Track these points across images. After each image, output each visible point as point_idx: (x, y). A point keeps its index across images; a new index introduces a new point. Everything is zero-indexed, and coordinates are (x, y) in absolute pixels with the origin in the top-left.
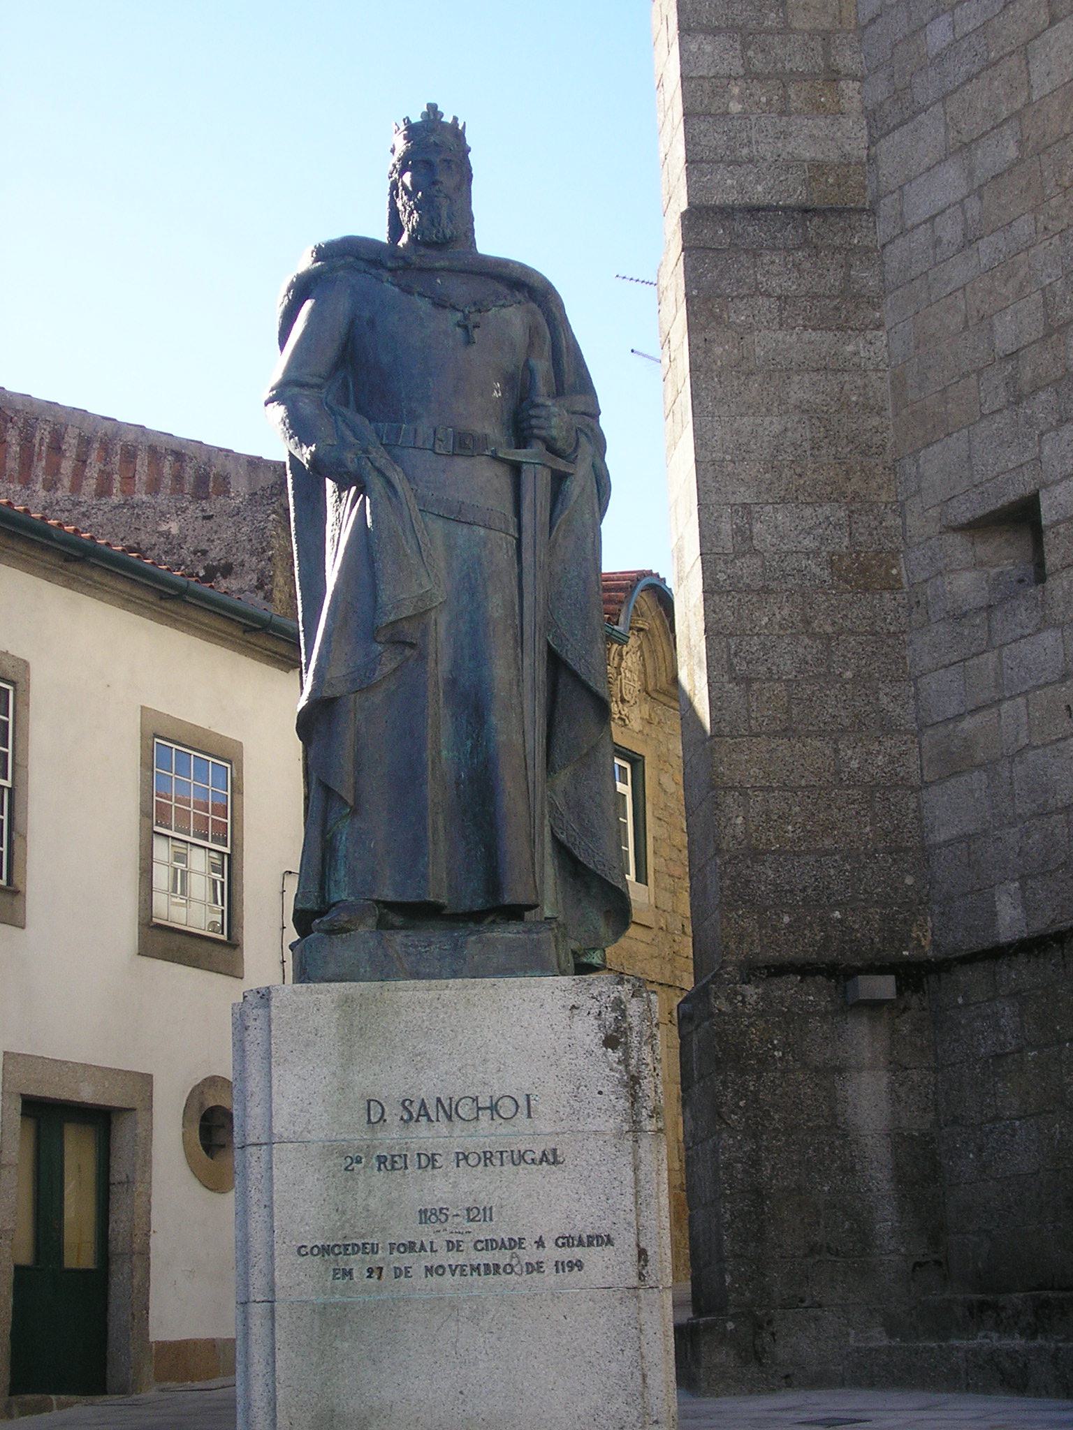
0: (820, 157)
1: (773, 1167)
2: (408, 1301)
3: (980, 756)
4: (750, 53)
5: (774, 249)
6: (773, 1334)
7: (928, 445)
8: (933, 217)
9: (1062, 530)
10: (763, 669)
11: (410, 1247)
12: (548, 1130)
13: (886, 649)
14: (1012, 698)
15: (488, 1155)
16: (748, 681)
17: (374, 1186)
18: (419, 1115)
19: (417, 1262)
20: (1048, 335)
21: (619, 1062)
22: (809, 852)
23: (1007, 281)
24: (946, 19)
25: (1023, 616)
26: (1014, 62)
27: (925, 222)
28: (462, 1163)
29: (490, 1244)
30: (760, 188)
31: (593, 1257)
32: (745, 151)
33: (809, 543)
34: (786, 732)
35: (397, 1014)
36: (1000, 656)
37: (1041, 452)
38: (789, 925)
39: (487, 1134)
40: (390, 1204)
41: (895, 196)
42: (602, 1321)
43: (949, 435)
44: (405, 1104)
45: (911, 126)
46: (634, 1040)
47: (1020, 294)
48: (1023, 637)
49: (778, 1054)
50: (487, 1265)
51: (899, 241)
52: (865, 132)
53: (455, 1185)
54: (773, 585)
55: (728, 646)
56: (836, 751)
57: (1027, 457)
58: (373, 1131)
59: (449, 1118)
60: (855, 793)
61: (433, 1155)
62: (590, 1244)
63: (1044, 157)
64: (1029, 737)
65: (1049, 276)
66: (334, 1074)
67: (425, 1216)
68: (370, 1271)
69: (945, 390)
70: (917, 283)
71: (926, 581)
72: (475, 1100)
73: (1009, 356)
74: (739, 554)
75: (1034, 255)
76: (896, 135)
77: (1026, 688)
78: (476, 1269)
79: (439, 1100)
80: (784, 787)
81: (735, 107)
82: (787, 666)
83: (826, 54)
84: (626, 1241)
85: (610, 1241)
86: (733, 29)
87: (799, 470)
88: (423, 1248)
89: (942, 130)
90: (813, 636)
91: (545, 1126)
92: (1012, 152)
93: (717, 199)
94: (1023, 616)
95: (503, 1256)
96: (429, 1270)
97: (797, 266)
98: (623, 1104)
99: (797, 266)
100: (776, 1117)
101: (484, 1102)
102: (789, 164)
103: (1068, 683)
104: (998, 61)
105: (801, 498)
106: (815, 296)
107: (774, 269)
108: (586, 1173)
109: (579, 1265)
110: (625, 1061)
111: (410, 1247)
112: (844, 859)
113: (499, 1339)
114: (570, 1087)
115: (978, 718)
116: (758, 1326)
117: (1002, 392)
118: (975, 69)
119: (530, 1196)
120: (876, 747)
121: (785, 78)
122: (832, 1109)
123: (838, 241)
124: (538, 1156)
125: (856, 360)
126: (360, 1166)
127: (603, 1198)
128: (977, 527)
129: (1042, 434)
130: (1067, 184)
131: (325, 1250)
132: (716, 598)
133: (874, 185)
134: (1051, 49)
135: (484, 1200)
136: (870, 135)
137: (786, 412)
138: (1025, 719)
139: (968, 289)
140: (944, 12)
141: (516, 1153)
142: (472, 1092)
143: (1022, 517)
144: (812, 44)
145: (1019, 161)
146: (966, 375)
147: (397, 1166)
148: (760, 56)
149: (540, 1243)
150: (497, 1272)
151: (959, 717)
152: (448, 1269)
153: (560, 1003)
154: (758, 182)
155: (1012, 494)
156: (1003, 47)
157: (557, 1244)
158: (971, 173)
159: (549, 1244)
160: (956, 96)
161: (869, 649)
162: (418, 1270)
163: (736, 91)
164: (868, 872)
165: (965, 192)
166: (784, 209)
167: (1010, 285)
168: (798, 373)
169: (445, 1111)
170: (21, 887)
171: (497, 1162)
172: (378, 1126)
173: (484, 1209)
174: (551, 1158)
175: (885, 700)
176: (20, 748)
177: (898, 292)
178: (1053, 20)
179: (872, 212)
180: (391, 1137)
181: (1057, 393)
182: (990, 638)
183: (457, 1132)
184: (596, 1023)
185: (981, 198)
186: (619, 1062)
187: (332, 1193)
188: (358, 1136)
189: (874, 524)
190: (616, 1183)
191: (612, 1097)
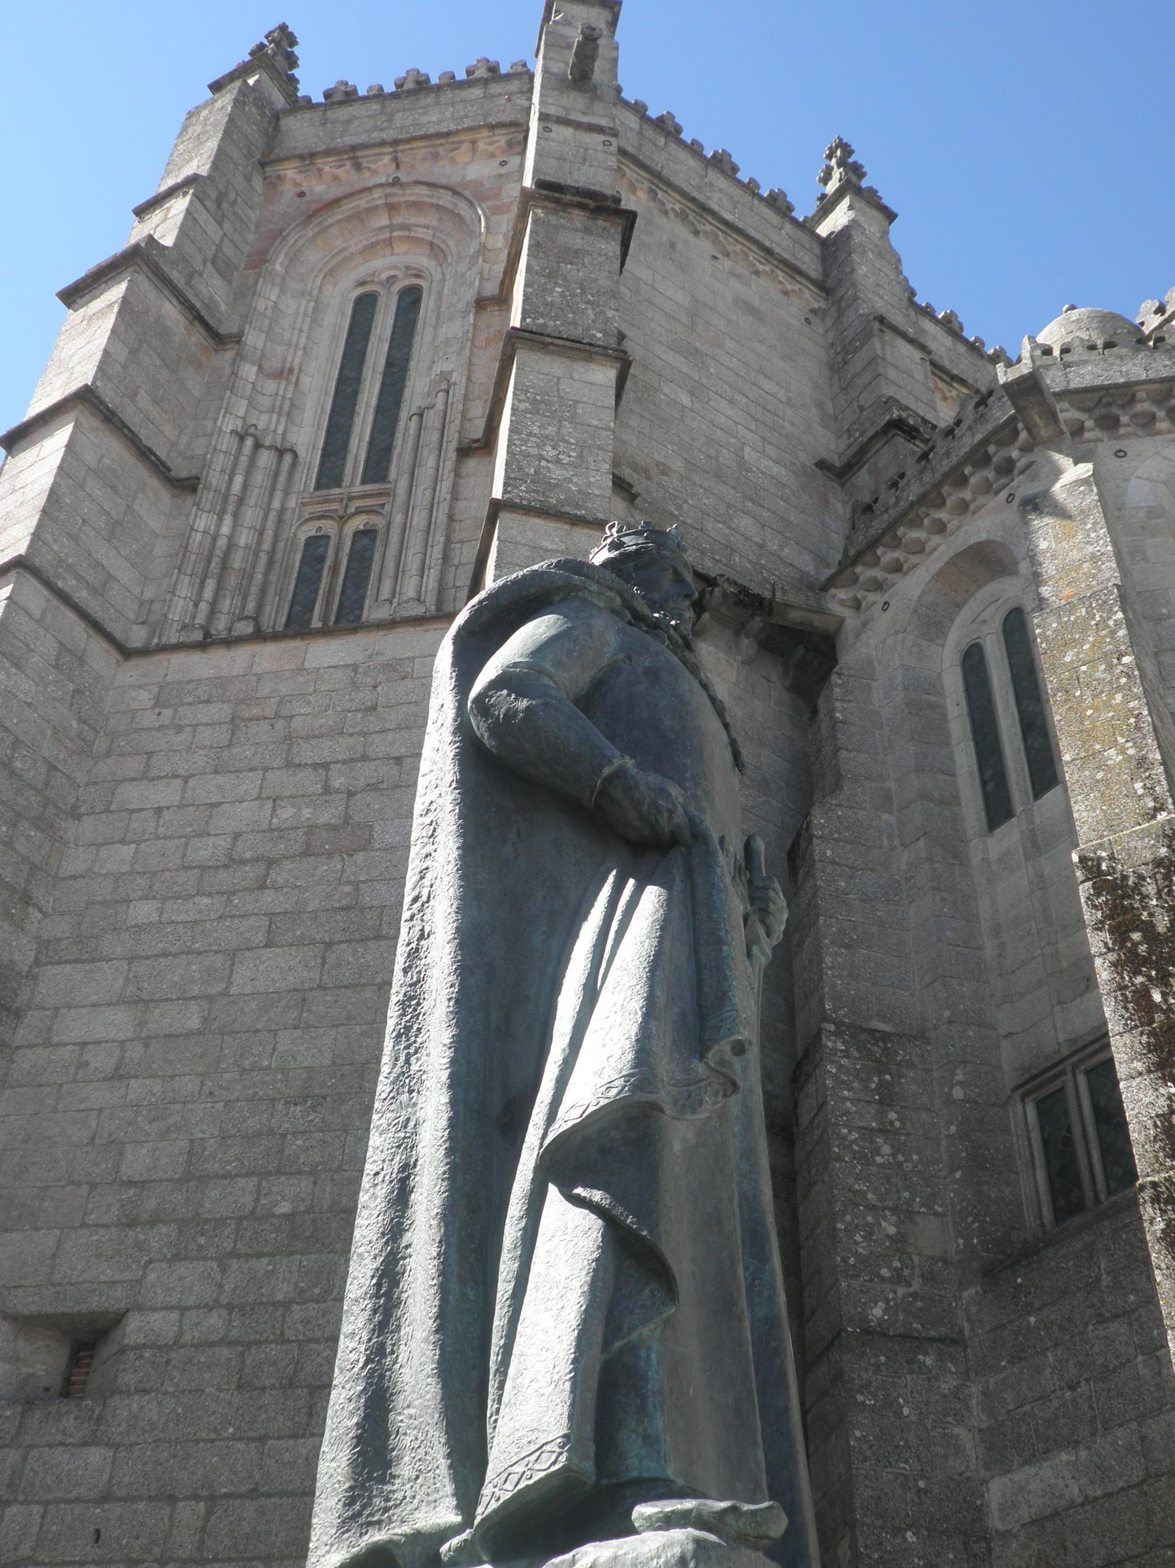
8: (85, 1044)
9: (147, 1355)
14: (25, 1503)
23: (154, 1120)
25: (70, 1423)
26: (219, 958)
27: (75, 1044)
37: (144, 1276)
41: (48, 1013)
43: (36, 1229)
48: (62, 1444)
51: (40, 1050)
52: (33, 954)
57: (127, 1276)
64: (34, 1549)
65: (203, 1132)
69: (46, 1188)
70: (47, 1090)
73: (131, 1183)
75: (192, 1110)
76: (68, 968)
77: (49, 1497)
83: (28, 882)
89: (121, 982)
92: (194, 1023)
94: (70, 1423)
103: (106, 1506)
104: (200, 953)
117: (115, 1212)
118: (174, 950)
128: (27, 1324)
129: (151, 1261)
130: (247, 1067)
133: (26, 997)
134: (262, 962)
136: (37, 958)
138: (35, 1529)
139: (105, 1113)
140: (154, 898)
144: (22, 867)
145: (199, 1032)
146: (79, 1184)
155: (95, 1303)
156: (210, 945)
158: (141, 1024)
165: (129, 1035)
167: (155, 1125)
177: (21, 1090)
179: (18, 1014)
181: (180, 1231)
182: (18, 1433)
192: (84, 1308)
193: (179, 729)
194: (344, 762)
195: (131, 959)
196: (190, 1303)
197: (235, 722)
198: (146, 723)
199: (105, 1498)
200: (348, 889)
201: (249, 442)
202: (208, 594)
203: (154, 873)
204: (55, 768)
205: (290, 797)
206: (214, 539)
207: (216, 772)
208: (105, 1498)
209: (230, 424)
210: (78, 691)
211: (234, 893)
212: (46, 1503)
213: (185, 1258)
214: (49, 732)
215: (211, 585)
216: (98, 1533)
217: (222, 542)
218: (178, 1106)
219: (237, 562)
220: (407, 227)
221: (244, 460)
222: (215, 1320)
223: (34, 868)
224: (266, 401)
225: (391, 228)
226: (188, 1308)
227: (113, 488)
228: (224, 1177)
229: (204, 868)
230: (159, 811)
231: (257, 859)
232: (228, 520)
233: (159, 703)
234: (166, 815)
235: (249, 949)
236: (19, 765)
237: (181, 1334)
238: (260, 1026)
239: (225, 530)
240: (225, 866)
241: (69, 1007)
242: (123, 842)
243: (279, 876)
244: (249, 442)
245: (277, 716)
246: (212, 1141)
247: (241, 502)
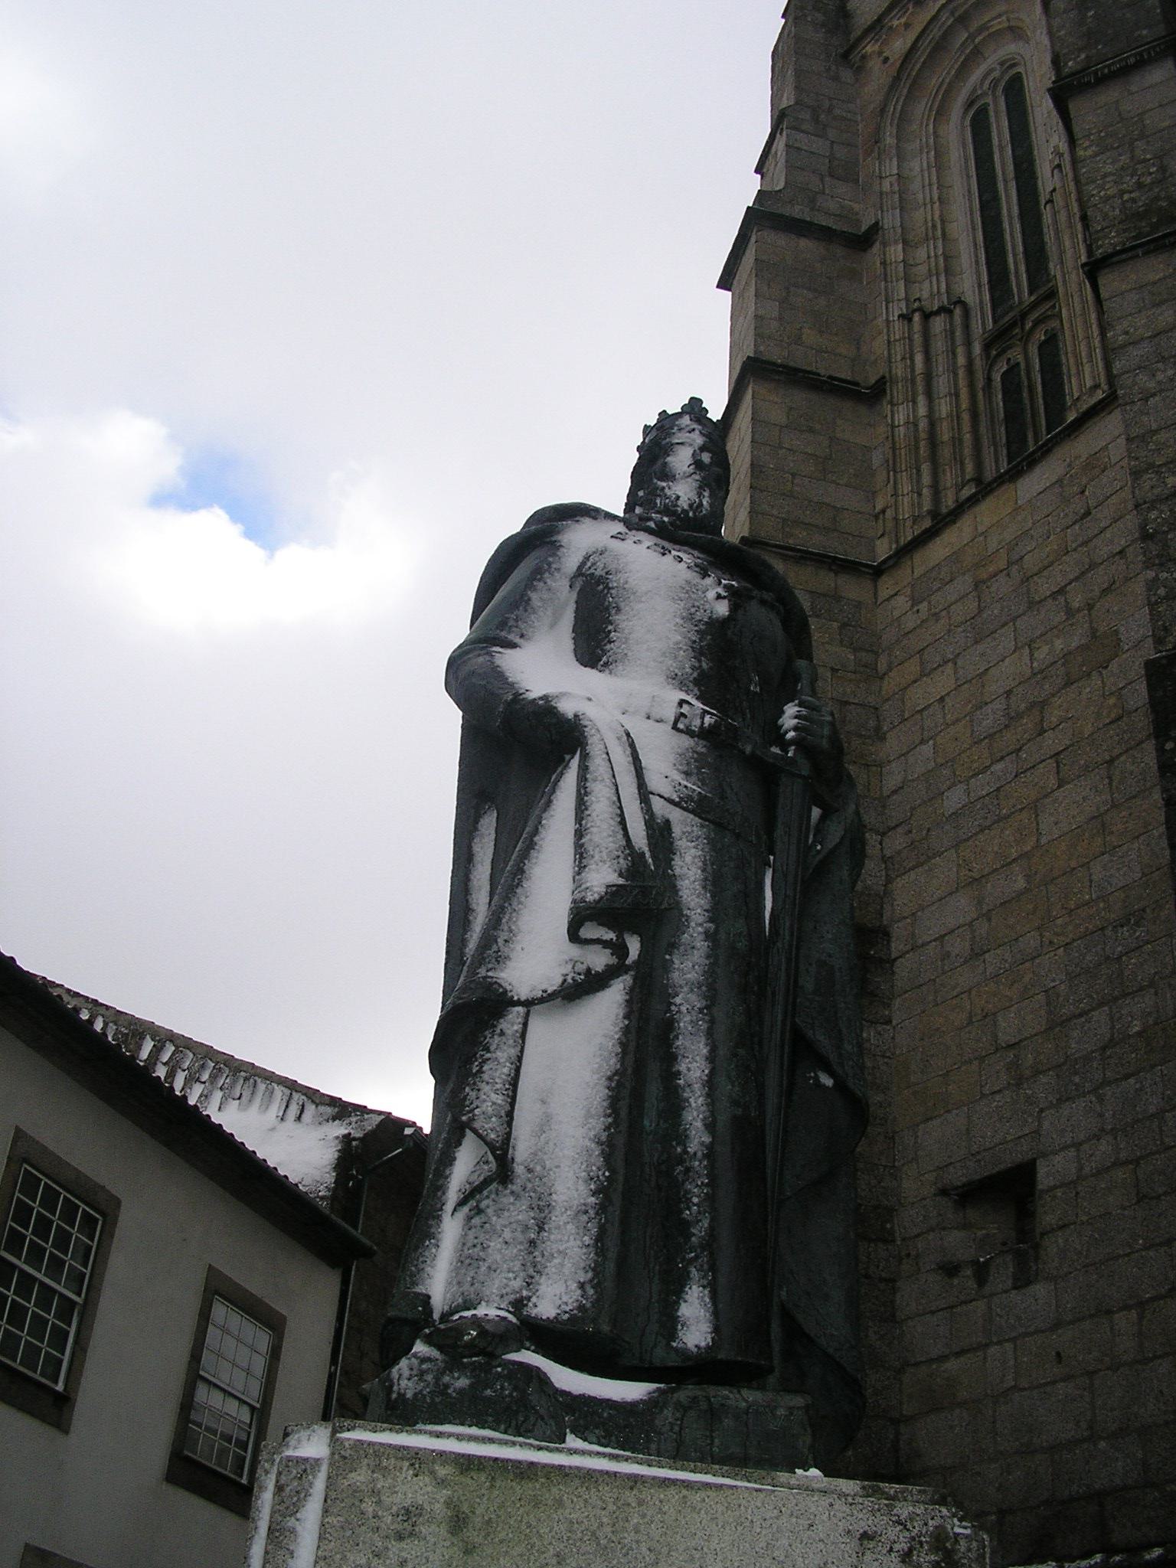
7: (928, 1120)
14: (999, 1343)
20: (1051, 1028)
24: (962, 787)
26: (1025, 815)
36: (990, 1308)
37: (1040, 1125)
43: (948, 1111)
63: (1051, 888)
65: (1053, 980)
70: (924, 988)
71: (918, 1236)
73: (1011, 1046)
77: (1014, 1334)
92: (1021, 883)
118: (988, 823)
129: (1042, 1111)
138: (1012, 1362)
139: (974, 992)
145: (1027, 890)
146: (970, 1062)
151: (943, 1358)
155: (1008, 1160)
178: (1061, 784)
185: (989, 920)
189: (874, 1182)
193: (936, 616)
194: (1076, 579)
195: (956, 846)
196: (1082, 1137)
197: (977, 584)
198: (910, 625)
199: (1057, 1325)
200: (1112, 701)
201: (917, 317)
202: (926, 479)
203: (953, 760)
204: (847, 703)
205: (1042, 635)
206: (916, 425)
207: (976, 642)
208: (1057, 1325)
209: (898, 308)
210: (844, 625)
211: (1020, 749)
212: (1013, 1340)
213: (1068, 1099)
214: (829, 674)
215: (926, 468)
216: (1058, 1354)
217: (923, 424)
218: (1027, 964)
219: (945, 434)
220: (980, 30)
221: (918, 338)
222: (1104, 1146)
224: (922, 270)
225: (971, 37)
226: (1080, 1144)
227: (811, 430)
228: (1081, 1015)
229: (991, 736)
230: (942, 699)
232: (921, 400)
233: (915, 601)
235: (1046, 796)
237: (1081, 1168)
238: (1073, 864)
239: (922, 411)
241: (922, 909)
242: (923, 742)
243: (1053, 716)
244: (917, 317)
245: (1010, 564)
246: (1063, 987)
247: (928, 377)
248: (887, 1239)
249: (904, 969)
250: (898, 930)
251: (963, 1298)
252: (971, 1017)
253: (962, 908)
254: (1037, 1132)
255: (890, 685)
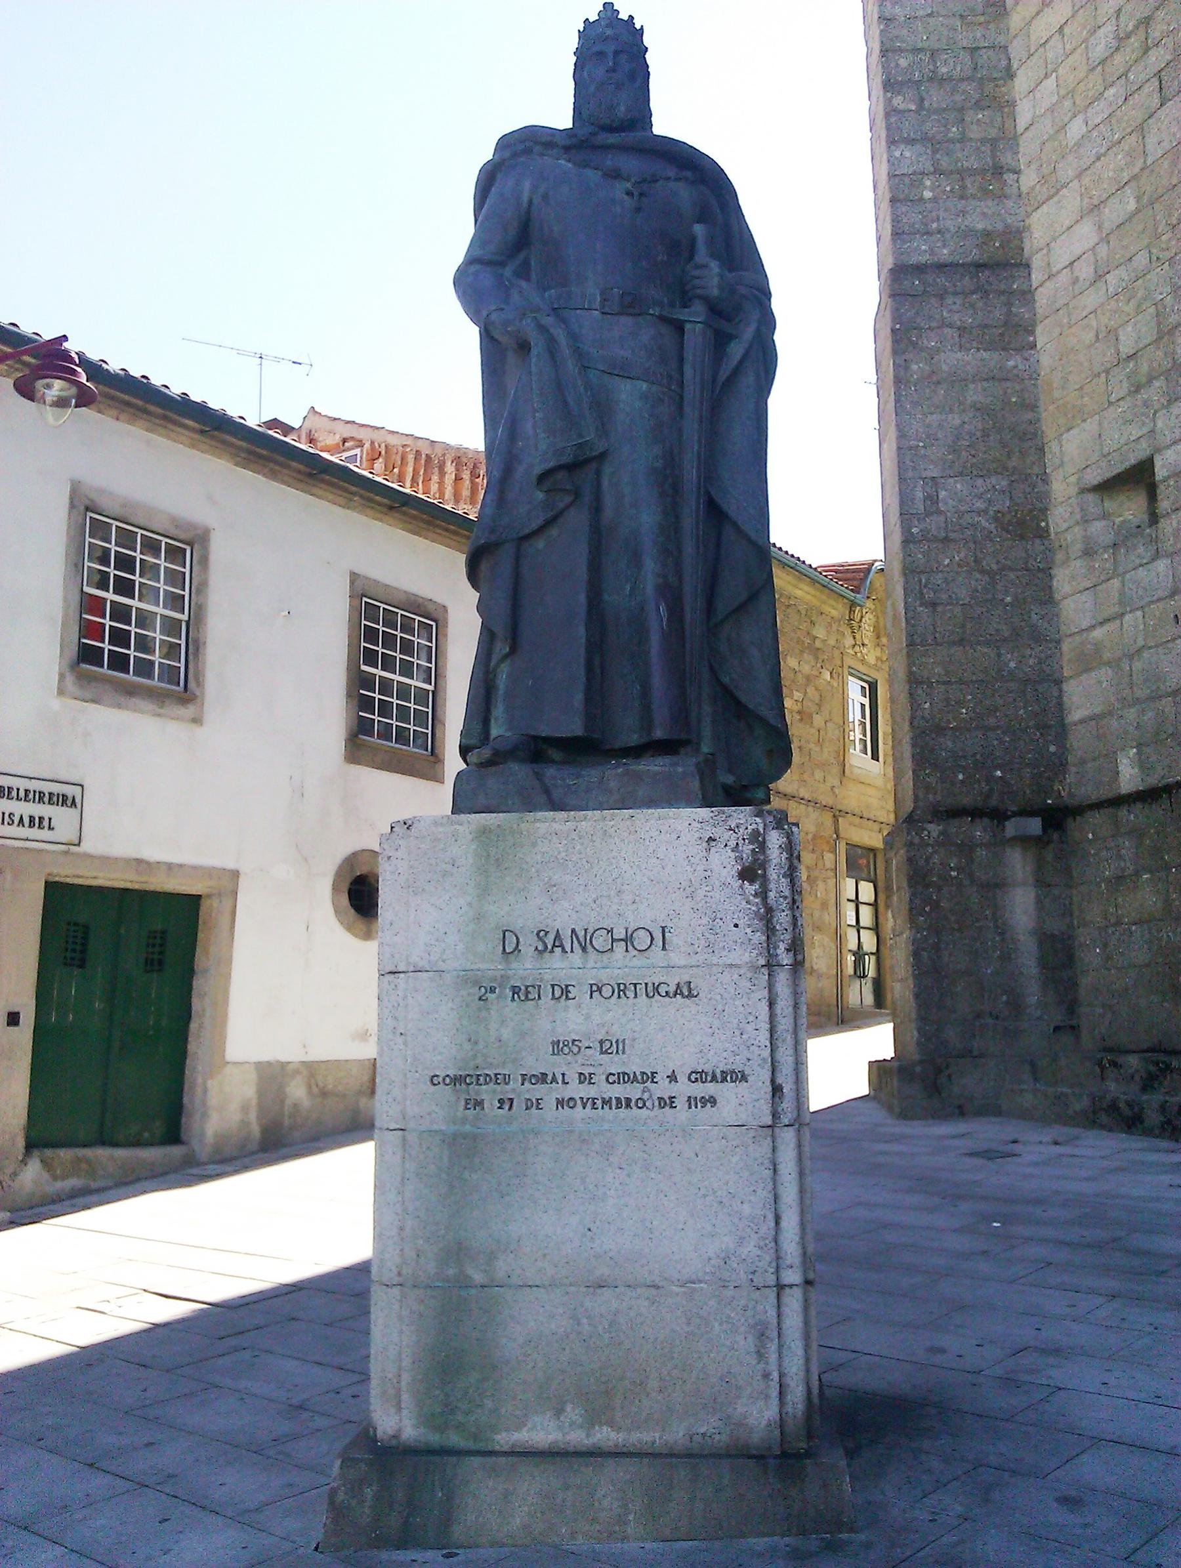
0: (989, 228)
1: (950, 955)
2: (536, 1133)
3: (1107, 655)
4: (938, 156)
5: (956, 294)
6: (949, 1076)
8: (1072, 264)
10: (945, 597)
11: (542, 1078)
12: (683, 963)
13: (1037, 581)
15: (622, 987)
16: (934, 605)
17: (506, 1016)
18: (554, 946)
19: (549, 1094)
20: (1159, 339)
21: (756, 895)
22: (977, 727)
24: (1080, 119)
26: (1134, 137)
28: (595, 994)
29: (623, 1078)
30: (945, 251)
31: (727, 1092)
32: (934, 225)
33: (980, 505)
34: (961, 642)
35: (534, 845)
36: (1123, 582)
37: (1155, 425)
38: (962, 782)
39: (621, 965)
40: (523, 1035)
41: (1045, 251)
42: (734, 1160)
43: (1084, 421)
44: (540, 935)
45: (1055, 199)
46: (773, 874)
47: (1139, 311)
48: (1141, 565)
49: (954, 874)
50: (618, 1099)
51: (1048, 284)
53: (588, 1017)
54: (953, 536)
55: (920, 581)
56: (999, 655)
57: (1145, 430)
58: (507, 961)
59: (584, 949)
60: (1013, 686)
61: (567, 986)
62: (724, 1080)
66: (470, 904)
67: (558, 1047)
68: (501, 1101)
69: (1081, 388)
72: (610, 931)
73: (1129, 357)
74: (928, 514)
77: (1143, 603)
78: (606, 1102)
79: (573, 931)
80: (961, 682)
81: (928, 194)
82: (963, 594)
83: (994, 156)
84: (760, 1078)
85: (744, 1078)
86: (926, 139)
87: (973, 452)
88: (554, 1080)
90: (982, 571)
91: (676, 958)
92: (1132, 205)
93: (914, 260)
94: (1141, 550)
95: (635, 1092)
96: (560, 1103)
97: (972, 306)
98: (759, 937)
99: (972, 306)
100: (953, 918)
101: (620, 933)
102: (967, 233)
105: (975, 473)
106: (986, 326)
107: (955, 307)
108: (720, 1007)
109: (713, 1101)
110: (763, 894)
111: (542, 1078)
112: (1004, 733)
113: (629, 1175)
114: (705, 920)
115: (1106, 627)
116: (939, 1071)
118: (1103, 151)
119: (662, 1029)
120: (1028, 652)
121: (962, 173)
122: (994, 914)
123: (1003, 287)
124: (672, 989)
125: (1015, 372)
126: (493, 996)
127: (737, 1033)
130: (1175, 222)
131: (457, 1080)
132: (911, 546)
135: (617, 1032)
137: (964, 411)
138: (1142, 627)
140: (1079, 112)
141: (650, 985)
142: (606, 924)
143: (1139, 477)
144: (983, 149)
145: (1138, 211)
146: (1099, 375)
147: (530, 997)
148: (945, 158)
149: (673, 1078)
150: (628, 1106)
152: (579, 1102)
153: (697, 835)
154: (944, 246)
157: (689, 1079)
159: (682, 1078)
160: (1089, 172)
161: (1024, 581)
162: (550, 1103)
163: (928, 183)
164: (1022, 742)
165: (1096, 240)
166: (963, 265)
168: (973, 382)
169: (579, 942)
170: (441, 757)
171: (631, 994)
172: (512, 957)
173: (617, 1042)
174: (685, 991)
175: (1034, 616)
176: (440, 663)
180: (525, 967)
183: (591, 964)
184: (733, 855)
186: (756, 895)
187: (465, 1022)
188: (492, 966)
189: (1028, 490)
190: (751, 1018)
191: (749, 930)
192: (1127, 465)
195: (1079, 176)
203: (1073, 91)
218: (1140, 281)
223: (993, 142)
229: (1103, 62)
231: (1137, 27)
234: (1067, 30)
236: (944, 70)
240: (1117, 49)
241: (1054, 239)
242: (1046, 76)
248: (1043, 534)
249: (1042, 298)
250: (1037, 262)
251: (1102, 578)
252: (1097, 336)
253: (1086, 233)
254: (1152, 431)
255: (1016, 20)
